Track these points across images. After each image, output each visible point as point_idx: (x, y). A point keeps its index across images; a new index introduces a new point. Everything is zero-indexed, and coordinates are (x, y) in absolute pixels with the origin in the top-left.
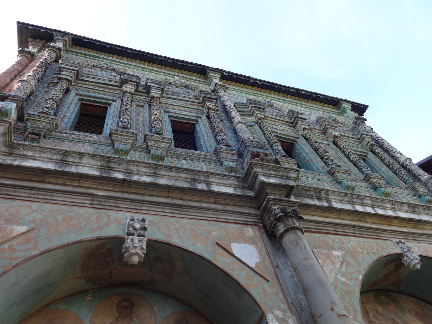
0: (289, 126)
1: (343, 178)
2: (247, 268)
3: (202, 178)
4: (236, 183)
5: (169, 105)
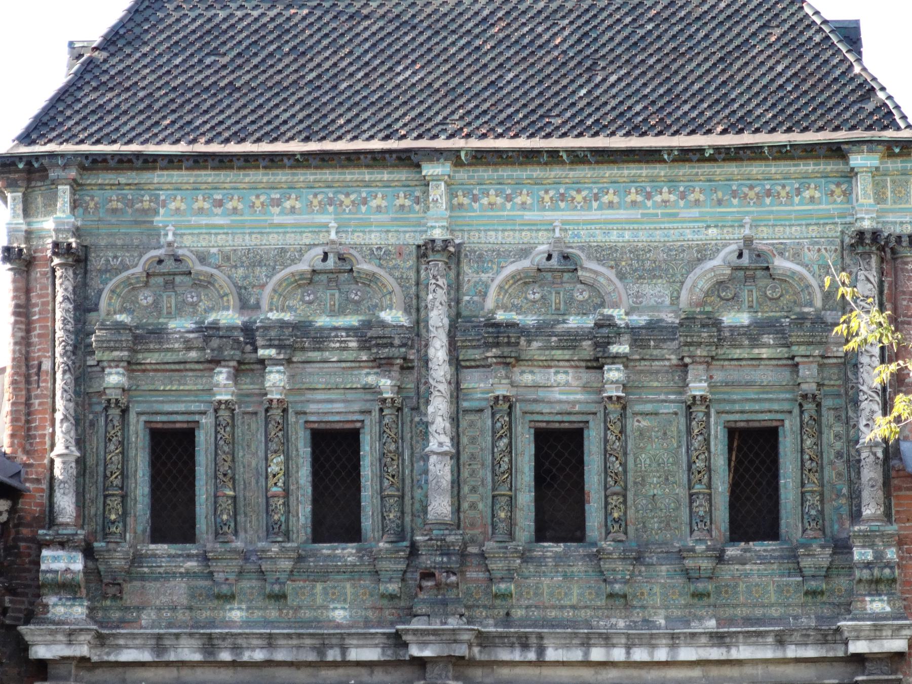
0: (588, 368)
3: (334, 641)
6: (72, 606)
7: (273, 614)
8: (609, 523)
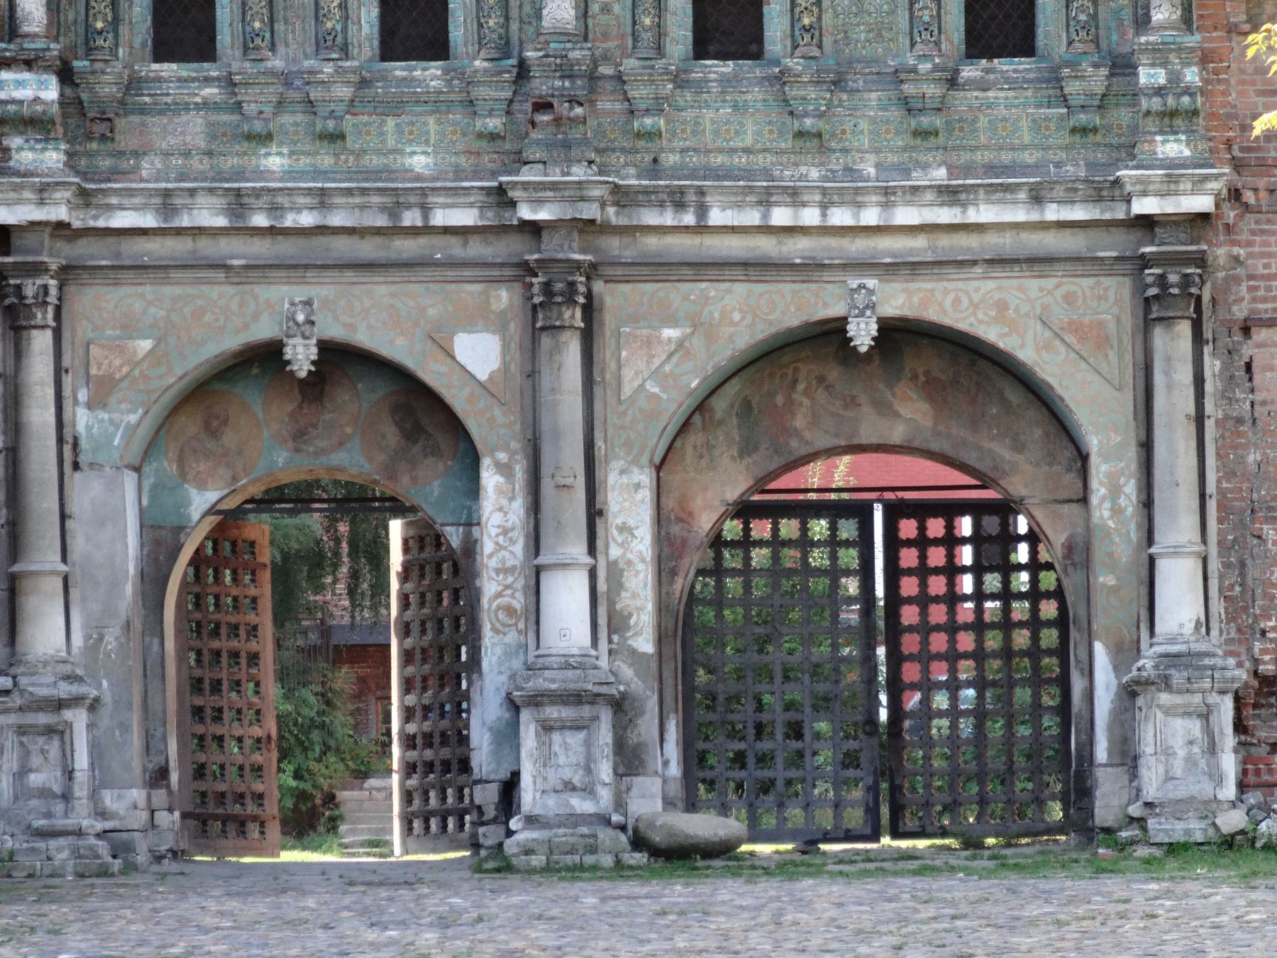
2: (474, 382)
3: (412, 199)
4: (485, 199)
6: (45, 149)
7: (326, 161)
8: (797, 33)
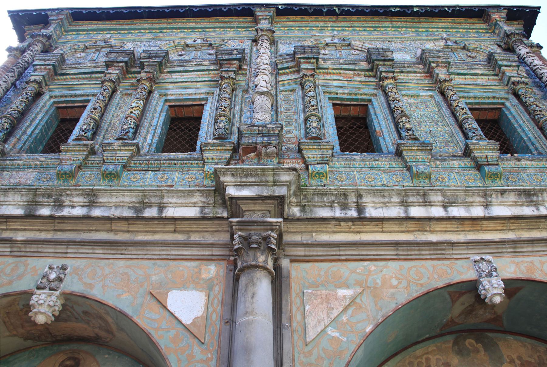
1: (416, 159)
2: (180, 326)
3: (153, 200)
4: (204, 200)
5: (170, 84)
